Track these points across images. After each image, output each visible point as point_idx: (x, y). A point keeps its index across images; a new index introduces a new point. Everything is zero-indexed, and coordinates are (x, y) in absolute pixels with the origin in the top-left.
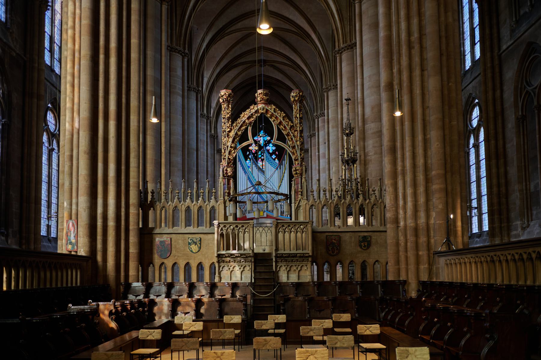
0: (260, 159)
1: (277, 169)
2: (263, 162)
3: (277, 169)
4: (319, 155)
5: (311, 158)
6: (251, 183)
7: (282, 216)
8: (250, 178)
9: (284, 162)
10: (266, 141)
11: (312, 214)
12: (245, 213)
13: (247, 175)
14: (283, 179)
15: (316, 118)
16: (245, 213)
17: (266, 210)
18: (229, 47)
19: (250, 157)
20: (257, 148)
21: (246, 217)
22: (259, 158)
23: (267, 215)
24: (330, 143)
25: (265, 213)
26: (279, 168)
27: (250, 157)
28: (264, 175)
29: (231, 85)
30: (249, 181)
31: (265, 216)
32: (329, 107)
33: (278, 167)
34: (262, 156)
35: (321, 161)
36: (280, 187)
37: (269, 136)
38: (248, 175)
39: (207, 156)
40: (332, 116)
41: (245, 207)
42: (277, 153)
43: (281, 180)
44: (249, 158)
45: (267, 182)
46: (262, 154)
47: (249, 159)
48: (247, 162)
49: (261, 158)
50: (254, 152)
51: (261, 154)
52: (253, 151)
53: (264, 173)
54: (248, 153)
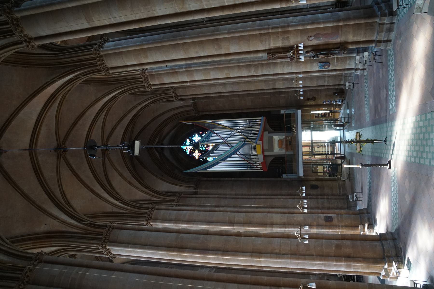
0: (207, 148)
1: (213, 132)
2: (210, 146)
3: (213, 132)
4: (190, 82)
5: (198, 95)
7: (261, 125)
8: (223, 159)
9: (206, 125)
10: (190, 143)
11: (258, 90)
12: (258, 163)
14: (223, 125)
15: (150, 87)
16: (258, 163)
17: (254, 142)
18: (81, 184)
19: (205, 158)
20: (197, 151)
21: (262, 163)
22: (206, 149)
23: (260, 141)
24: (166, 59)
25: (258, 143)
26: (213, 130)
27: (205, 158)
29: (128, 180)
31: (261, 142)
32: (125, 65)
33: (212, 131)
34: (204, 146)
35: (196, 79)
36: (231, 128)
37: (186, 140)
38: (220, 161)
39: (194, 211)
40: (133, 59)
42: (201, 133)
43: (224, 127)
44: (206, 158)
45: (226, 142)
46: (202, 146)
47: (207, 159)
48: (209, 160)
49: (206, 148)
50: (201, 154)
51: (202, 148)
52: (199, 155)
54: (201, 160)
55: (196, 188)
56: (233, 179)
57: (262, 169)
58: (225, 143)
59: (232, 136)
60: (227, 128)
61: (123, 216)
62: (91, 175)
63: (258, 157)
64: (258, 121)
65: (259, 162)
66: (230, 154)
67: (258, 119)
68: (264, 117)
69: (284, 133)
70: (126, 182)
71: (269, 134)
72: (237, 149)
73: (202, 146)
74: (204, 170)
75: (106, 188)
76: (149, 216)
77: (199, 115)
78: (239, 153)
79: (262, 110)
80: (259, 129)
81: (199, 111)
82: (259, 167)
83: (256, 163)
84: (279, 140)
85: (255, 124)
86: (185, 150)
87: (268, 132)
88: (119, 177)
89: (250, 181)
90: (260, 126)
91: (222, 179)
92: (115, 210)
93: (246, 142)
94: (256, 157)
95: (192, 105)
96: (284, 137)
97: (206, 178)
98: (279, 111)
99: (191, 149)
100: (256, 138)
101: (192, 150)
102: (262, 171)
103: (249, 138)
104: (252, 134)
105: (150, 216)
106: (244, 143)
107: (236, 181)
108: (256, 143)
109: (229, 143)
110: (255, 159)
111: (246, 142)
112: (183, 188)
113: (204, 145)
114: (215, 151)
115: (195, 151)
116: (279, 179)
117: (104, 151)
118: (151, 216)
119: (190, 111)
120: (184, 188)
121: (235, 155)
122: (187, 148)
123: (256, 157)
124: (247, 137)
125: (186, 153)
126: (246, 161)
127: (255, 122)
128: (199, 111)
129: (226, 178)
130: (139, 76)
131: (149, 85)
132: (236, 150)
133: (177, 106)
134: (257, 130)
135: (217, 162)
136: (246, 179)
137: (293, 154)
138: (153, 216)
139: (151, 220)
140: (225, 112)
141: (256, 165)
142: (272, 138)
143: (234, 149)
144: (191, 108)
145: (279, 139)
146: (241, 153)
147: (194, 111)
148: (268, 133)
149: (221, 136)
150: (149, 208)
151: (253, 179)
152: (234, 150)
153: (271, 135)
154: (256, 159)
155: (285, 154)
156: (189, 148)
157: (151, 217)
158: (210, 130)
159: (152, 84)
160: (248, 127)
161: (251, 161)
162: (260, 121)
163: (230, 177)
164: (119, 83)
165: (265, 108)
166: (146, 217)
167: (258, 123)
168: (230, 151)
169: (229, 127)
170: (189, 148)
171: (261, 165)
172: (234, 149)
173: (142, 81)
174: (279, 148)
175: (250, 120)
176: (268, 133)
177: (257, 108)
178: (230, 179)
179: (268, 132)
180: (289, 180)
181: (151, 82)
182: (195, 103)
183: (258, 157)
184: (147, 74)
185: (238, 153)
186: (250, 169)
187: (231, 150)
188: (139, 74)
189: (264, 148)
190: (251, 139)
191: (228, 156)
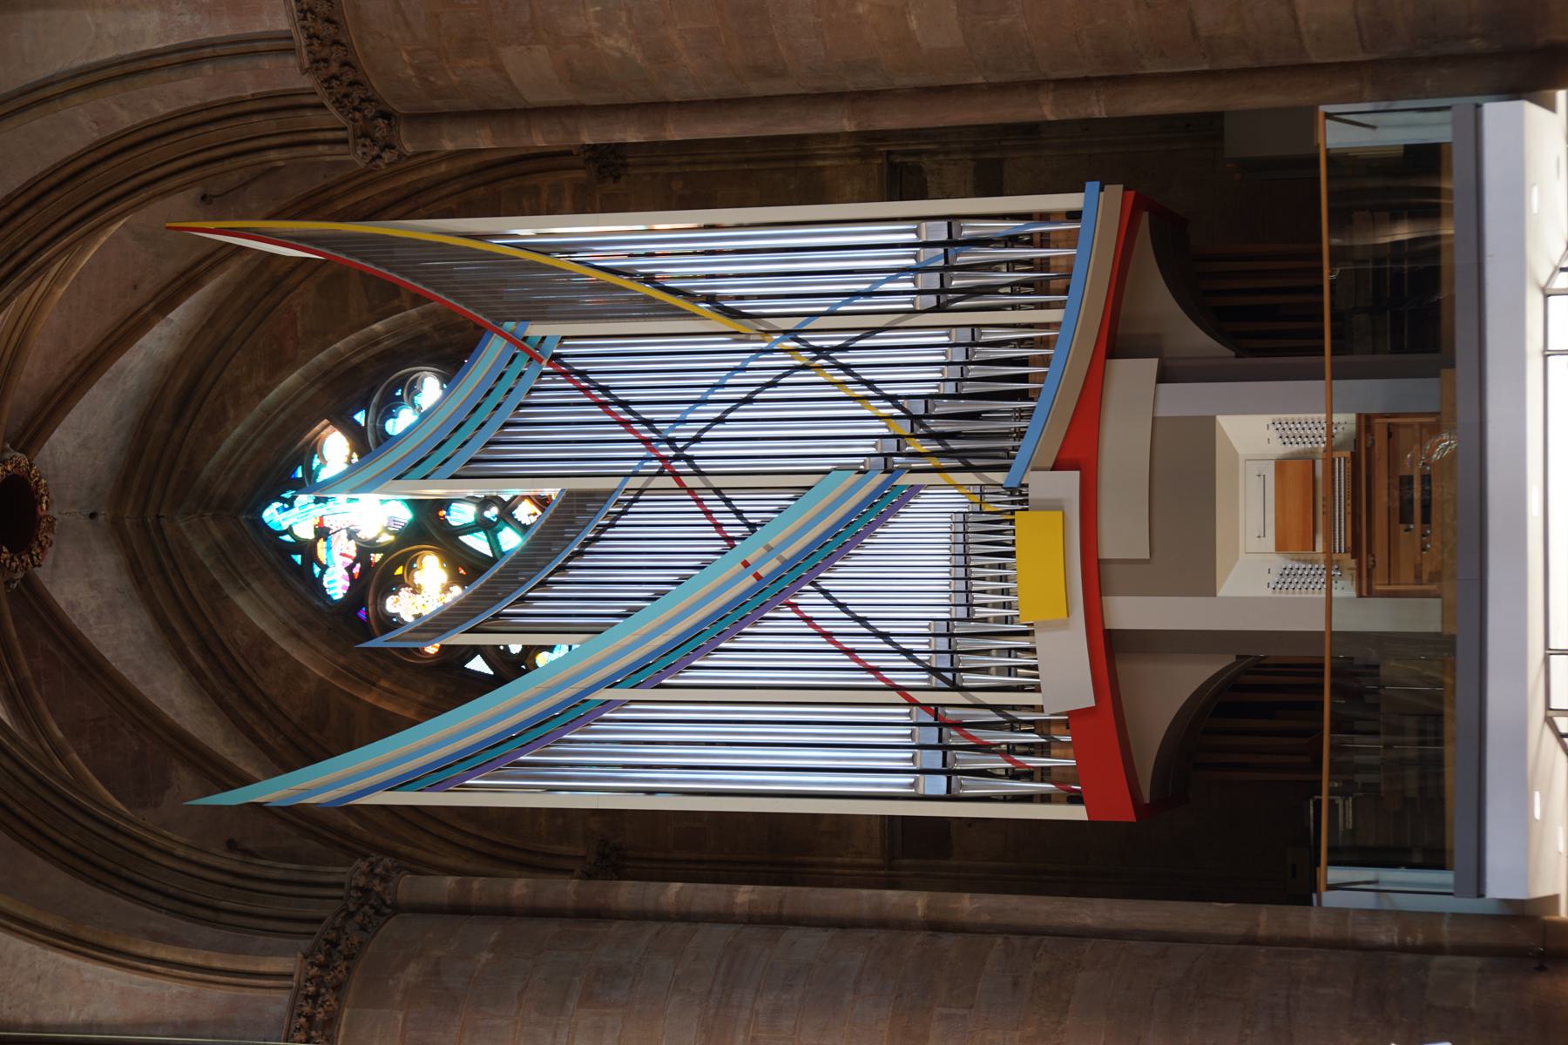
3: (531, 350)
6: (698, 652)
7: (1075, 283)
8: (640, 667)
12: (1036, 726)
13: (605, 694)
17: (998, 477)
21: (1074, 719)
23: (1056, 467)
25: (1033, 493)
26: (535, 330)
27: (515, 649)
28: (603, 496)
30: (669, 669)
36: (735, 314)
37: (314, 448)
41: (958, 725)
46: (492, 513)
53: (600, 497)
55: (314, 997)
56: (744, 895)
57: (1074, 799)
58: (669, 482)
59: (748, 400)
60: (693, 316)
63: (1031, 651)
64: (1044, 241)
65: (1040, 709)
66: (720, 616)
67: (1044, 217)
68: (1116, 191)
69: (1321, 383)
71: (1163, 386)
72: (807, 553)
73: (492, 513)
74: (432, 788)
77: (387, 156)
78: (819, 598)
79: (1097, 107)
80: (1057, 325)
81: (386, 115)
82: (1044, 774)
83: (1013, 725)
84: (1281, 464)
85: (1012, 265)
86: (308, 549)
87: (1153, 363)
89: (936, 926)
90: (1066, 292)
91: (627, 893)
93: (907, 480)
94: (1009, 652)
95: (300, 39)
96: (1345, 421)
97: (449, 882)
98: (1306, 120)
99: (365, 549)
100: (1020, 435)
101: (377, 557)
102: (1078, 813)
103: (939, 437)
104: (967, 388)
106: (879, 493)
107: (777, 921)
108: (1019, 495)
109: (717, 482)
110: (1000, 671)
111: (907, 480)
112: (172, 988)
113: (445, 504)
114: (561, 569)
115: (410, 570)
116: (1266, 919)
119: (281, 104)
120: (190, 988)
121: (781, 622)
122: (322, 532)
123: (1009, 652)
124: (914, 418)
125: (317, 586)
126: (894, 697)
127: (1012, 240)
128: (386, 115)
129: (675, 887)
132: (791, 565)
133: (128, 51)
134: (1021, 343)
135: (580, 700)
136: (892, 896)
137: (1435, 627)
140: (674, 132)
141: (1011, 750)
142: (1205, 430)
143: (762, 561)
144: (290, 75)
145: (1279, 450)
146: (842, 606)
147: (321, 106)
148: (1163, 377)
149: (624, 404)
151: (967, 905)
152: (774, 564)
153: (1183, 399)
154: (1009, 670)
155: (1322, 628)
156: (352, 535)
158: (509, 326)
160: (931, 300)
161: (956, 697)
162: (1071, 239)
163: (716, 880)
165: (1133, 79)
167: (1043, 265)
168: (727, 575)
169: (710, 299)
170: (352, 535)
171: (1077, 748)
172: (762, 561)
174: (1279, 562)
175: (951, 219)
176: (1163, 377)
177: (1034, 85)
178: (706, 895)
179: (1153, 363)
180: (1385, 935)
182: (329, 20)
183: (1031, 651)
185: (810, 601)
186: (938, 785)
187: (740, 567)
189: (1109, 548)
190: (955, 445)
191: (696, 632)
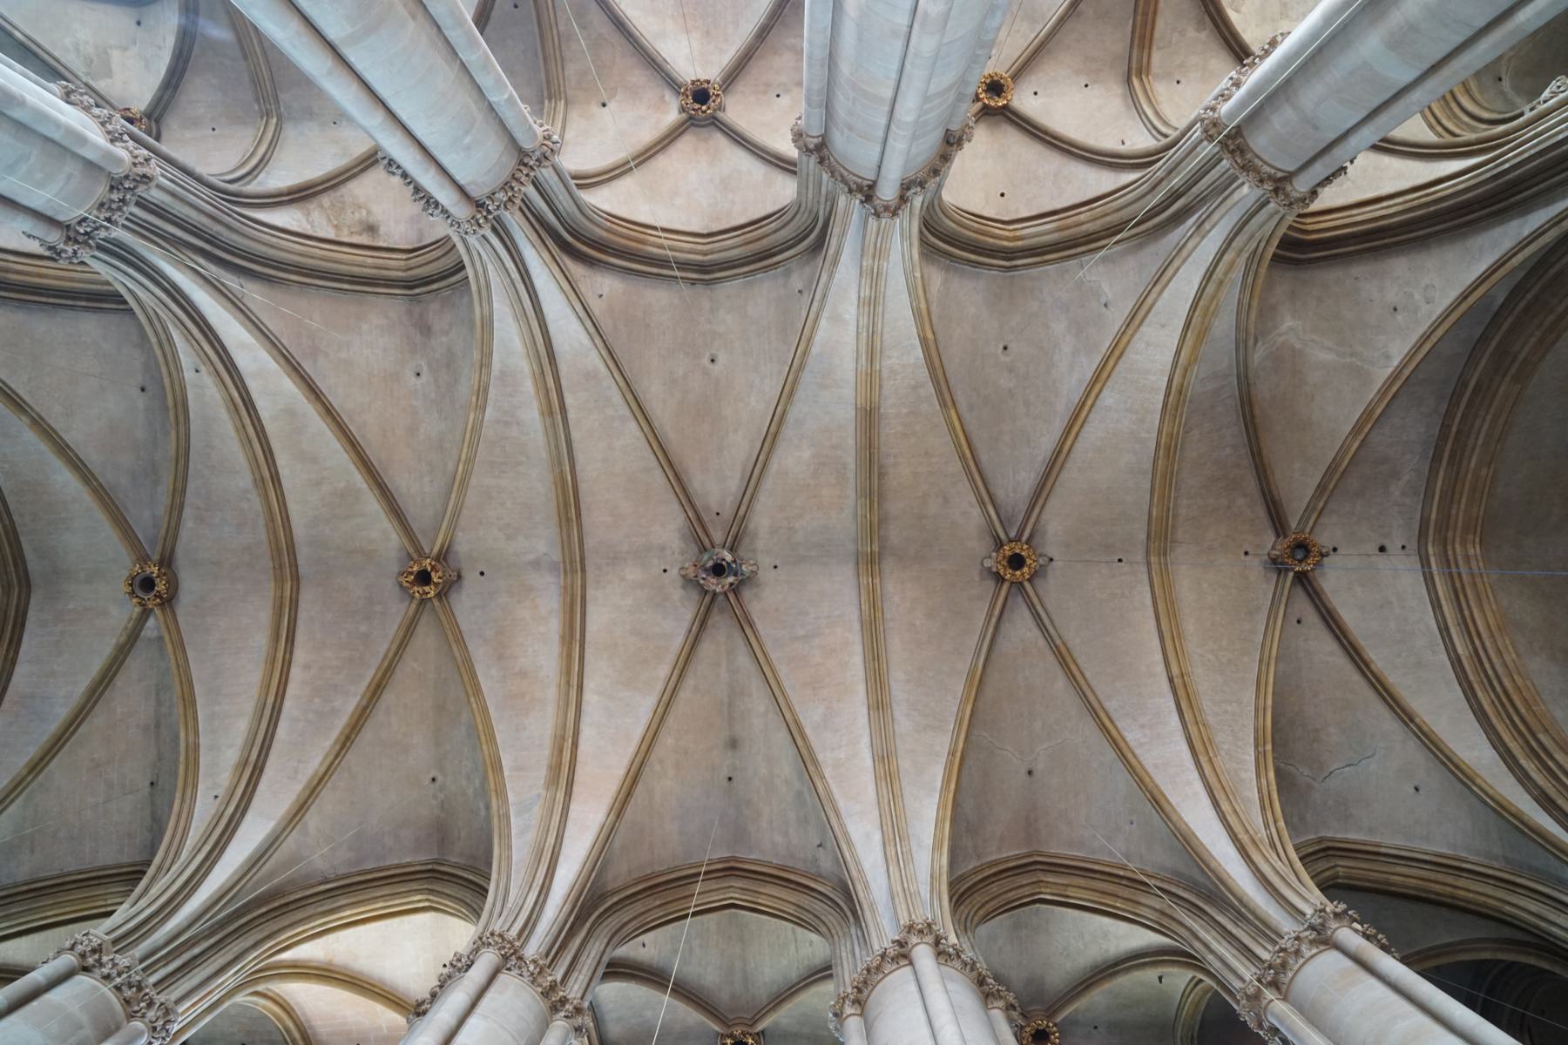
61: (212, 240)
62: (282, 461)
70: (37, 409)
75: (236, 395)
76: (123, 201)
88: (74, 436)
92: (231, 281)
105: (120, 200)
117: (164, 575)
118: (115, 196)
130: (174, 996)
131: (101, 965)
138: (101, 191)
139: (118, 171)
150: (100, 248)
157: (112, 188)
159: (82, 980)
164: (222, 924)
166: (138, 204)
173: (144, 970)
181: (95, 987)
184: (138, 1024)
188: (179, 1001)
